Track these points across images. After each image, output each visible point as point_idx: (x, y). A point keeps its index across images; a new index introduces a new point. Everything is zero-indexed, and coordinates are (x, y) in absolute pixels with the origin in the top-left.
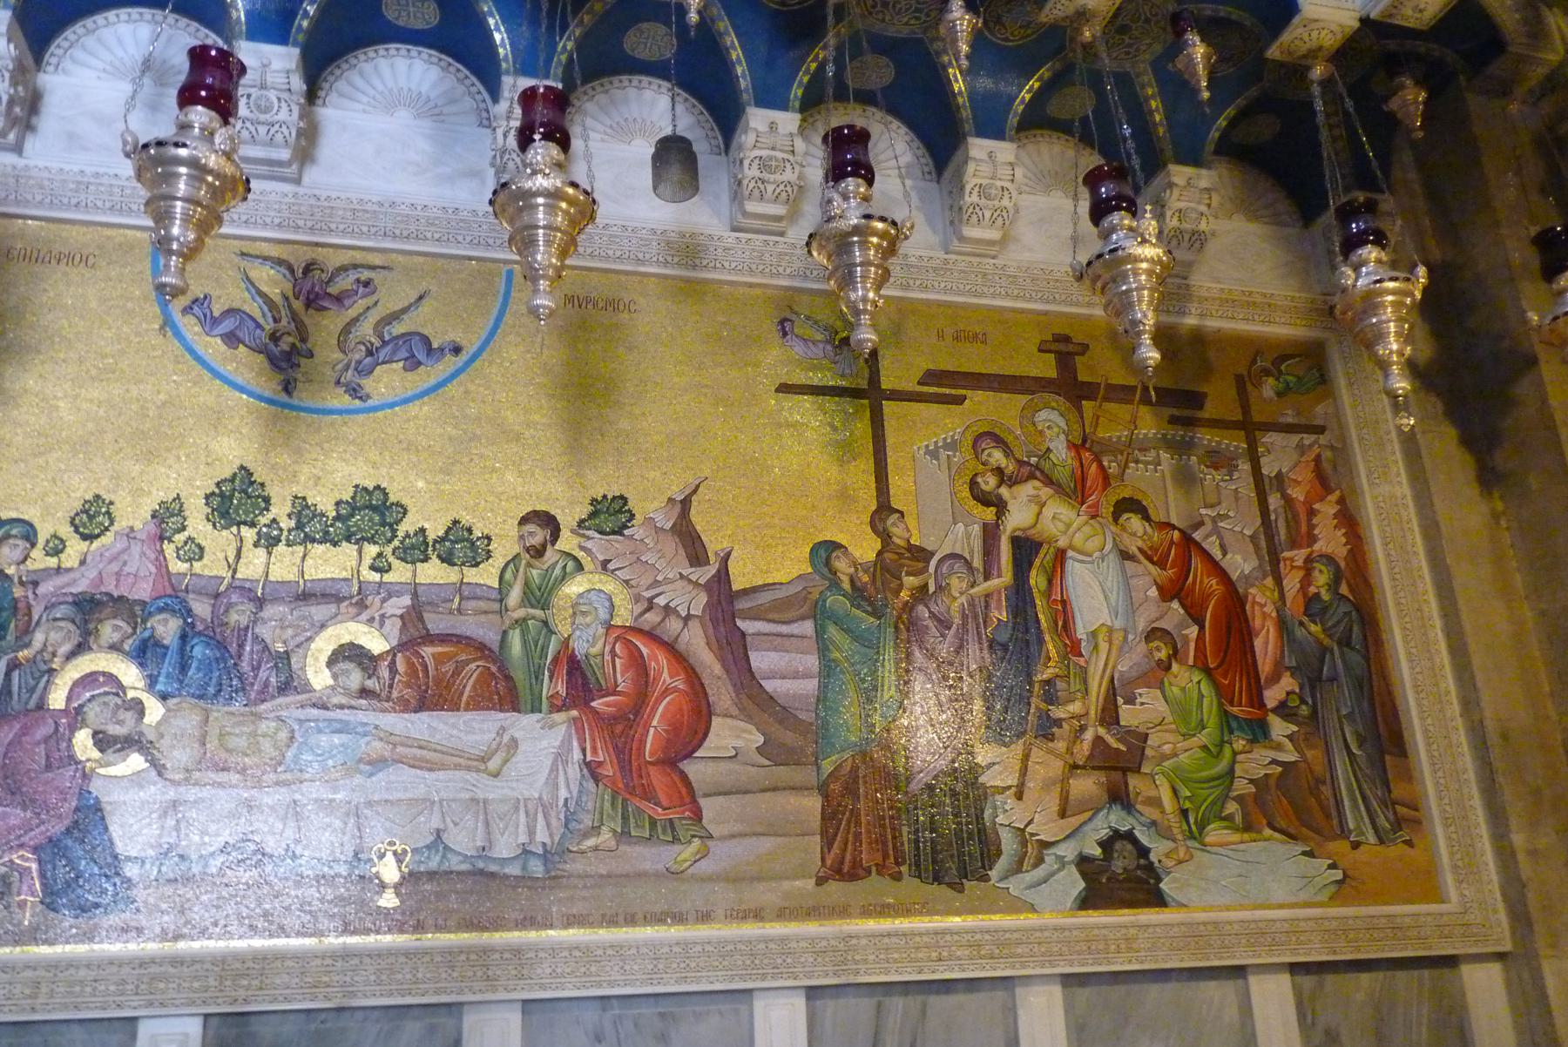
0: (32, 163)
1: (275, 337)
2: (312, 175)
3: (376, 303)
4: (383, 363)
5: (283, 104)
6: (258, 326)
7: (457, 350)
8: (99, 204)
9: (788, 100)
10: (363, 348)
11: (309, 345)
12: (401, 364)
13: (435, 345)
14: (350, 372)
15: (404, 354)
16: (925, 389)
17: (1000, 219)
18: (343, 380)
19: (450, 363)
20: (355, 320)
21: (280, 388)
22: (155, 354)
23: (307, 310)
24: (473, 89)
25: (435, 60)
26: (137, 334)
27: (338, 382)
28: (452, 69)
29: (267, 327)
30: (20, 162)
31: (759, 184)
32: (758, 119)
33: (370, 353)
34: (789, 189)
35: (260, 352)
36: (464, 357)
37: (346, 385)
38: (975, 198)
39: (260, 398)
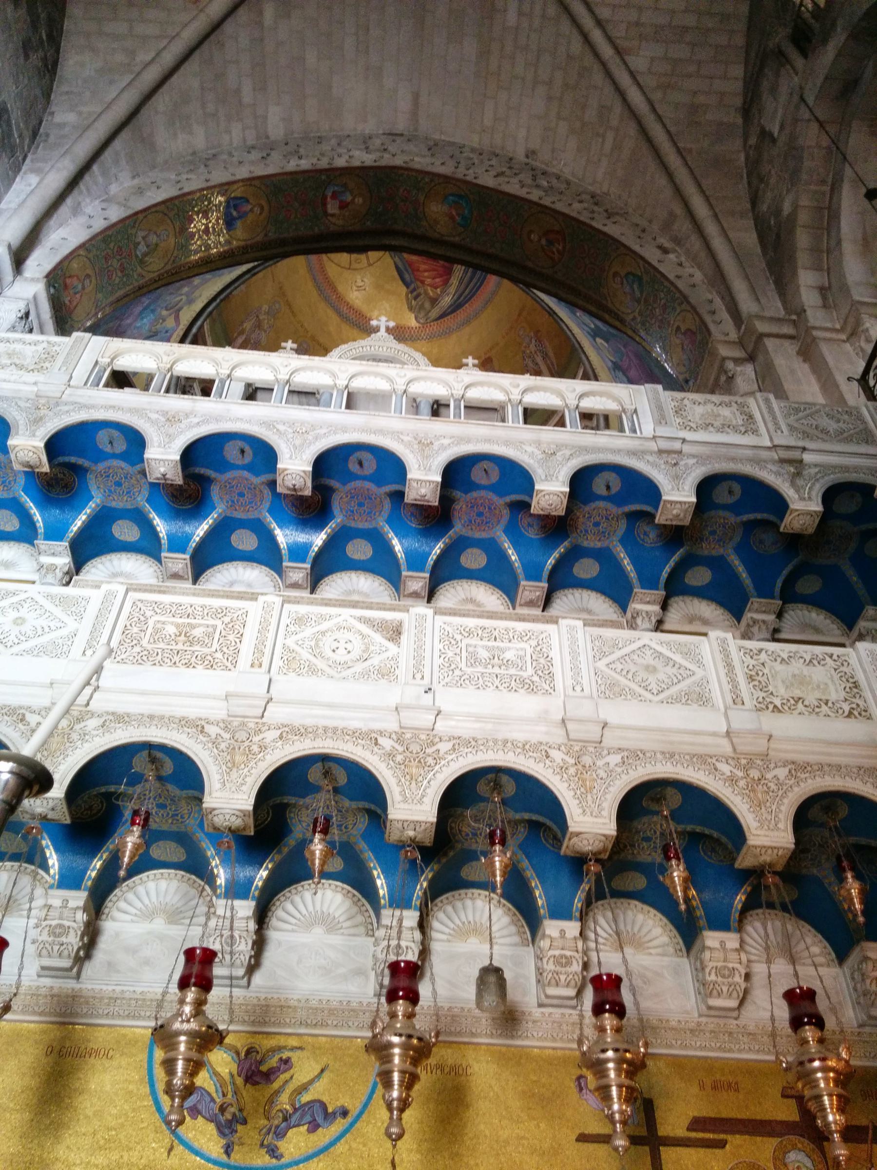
0: (83, 986)
1: (222, 1109)
2: (258, 978)
3: (292, 1077)
4: (294, 1126)
5: (243, 940)
6: (213, 1100)
7: (345, 1113)
8: (121, 1012)
9: (572, 912)
10: (281, 1115)
11: (245, 1114)
12: (306, 1127)
13: (330, 1110)
14: (271, 1135)
15: (308, 1118)
16: (693, 1135)
17: (735, 992)
18: (265, 1142)
19: (339, 1125)
20: (277, 1092)
21: (222, 1151)
22: (142, 1126)
23: (245, 1085)
24: (364, 909)
25: (339, 889)
26: (134, 1110)
27: (262, 1145)
28: (350, 895)
29: (218, 1100)
30: (77, 986)
31: (555, 975)
32: (552, 927)
33: (285, 1119)
34: (576, 977)
35: (212, 1121)
36: (349, 1119)
37: (267, 1147)
38: (713, 977)
39: (209, 1160)
